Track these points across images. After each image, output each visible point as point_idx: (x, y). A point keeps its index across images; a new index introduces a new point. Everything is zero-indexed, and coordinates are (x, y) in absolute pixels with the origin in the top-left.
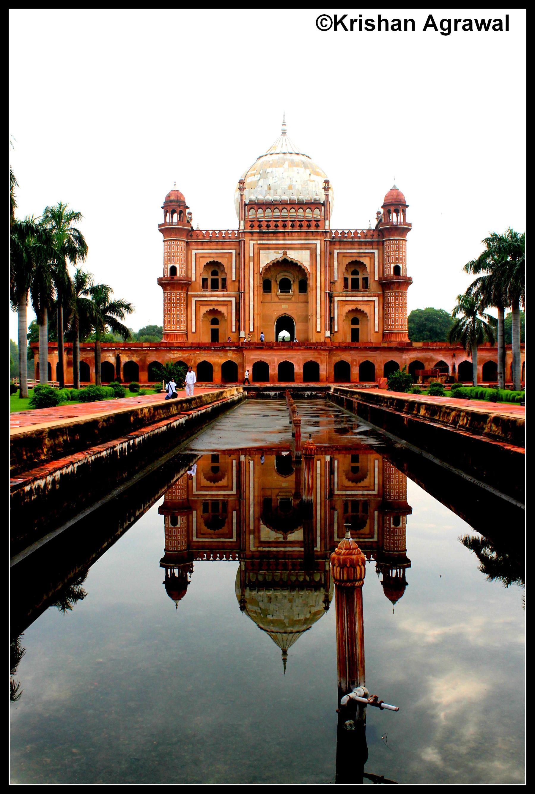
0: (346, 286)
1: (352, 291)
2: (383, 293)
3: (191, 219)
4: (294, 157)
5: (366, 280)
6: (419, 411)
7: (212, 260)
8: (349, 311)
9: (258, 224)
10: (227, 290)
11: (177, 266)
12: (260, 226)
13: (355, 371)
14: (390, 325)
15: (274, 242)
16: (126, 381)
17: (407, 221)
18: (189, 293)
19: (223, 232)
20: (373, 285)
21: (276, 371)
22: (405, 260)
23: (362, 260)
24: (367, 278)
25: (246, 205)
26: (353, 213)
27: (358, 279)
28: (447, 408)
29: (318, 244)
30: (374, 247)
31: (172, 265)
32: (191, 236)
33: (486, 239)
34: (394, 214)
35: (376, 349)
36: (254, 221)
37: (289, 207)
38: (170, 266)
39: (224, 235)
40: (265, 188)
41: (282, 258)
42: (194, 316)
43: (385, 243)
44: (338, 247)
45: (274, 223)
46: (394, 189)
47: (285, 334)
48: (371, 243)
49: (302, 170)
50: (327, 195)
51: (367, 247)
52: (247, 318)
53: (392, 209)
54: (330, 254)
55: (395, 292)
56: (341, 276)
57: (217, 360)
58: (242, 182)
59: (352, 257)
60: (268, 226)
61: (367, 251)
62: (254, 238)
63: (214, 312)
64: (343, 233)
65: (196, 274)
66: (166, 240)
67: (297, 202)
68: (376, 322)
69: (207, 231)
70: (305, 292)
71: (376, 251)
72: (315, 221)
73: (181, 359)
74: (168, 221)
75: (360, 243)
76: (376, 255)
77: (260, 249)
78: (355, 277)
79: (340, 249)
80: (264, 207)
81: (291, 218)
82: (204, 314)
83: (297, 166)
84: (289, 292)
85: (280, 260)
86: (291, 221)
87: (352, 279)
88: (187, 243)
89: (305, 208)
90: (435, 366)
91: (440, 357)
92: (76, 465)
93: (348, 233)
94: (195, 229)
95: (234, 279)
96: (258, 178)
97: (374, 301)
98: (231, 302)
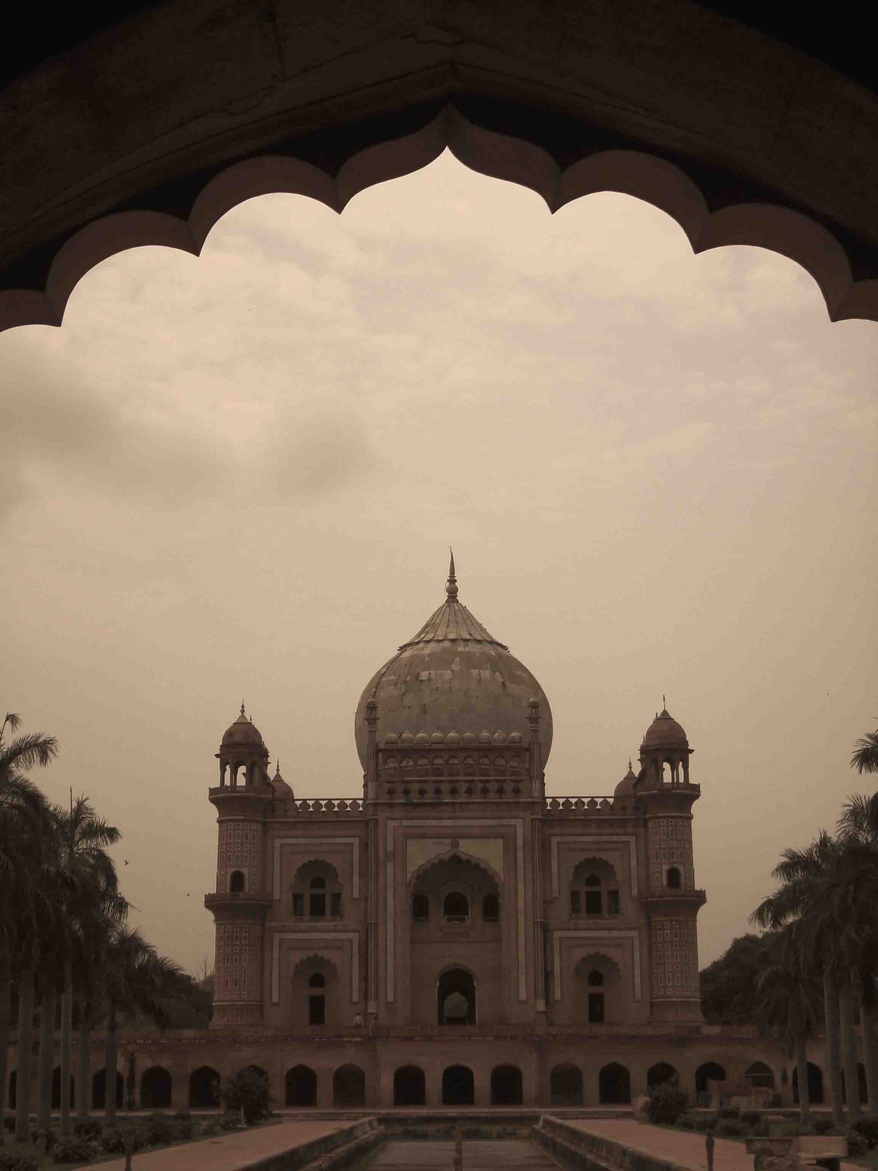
0: (575, 909)
8: (583, 959)
9: (400, 787)
11: (245, 871)
12: (407, 792)
13: (591, 1084)
15: (435, 822)
16: (144, 1106)
17: (692, 781)
18: (267, 924)
19: (336, 803)
21: (439, 1085)
23: (603, 856)
24: (617, 892)
25: (379, 750)
26: (586, 764)
27: (599, 894)
29: (520, 827)
30: (630, 830)
31: (234, 870)
33: (777, 870)
34: (666, 766)
38: (231, 871)
39: (336, 809)
42: (275, 970)
44: (557, 830)
46: (665, 718)
47: (456, 999)
48: (622, 823)
49: (486, 674)
50: (535, 731)
52: (381, 972)
54: (543, 845)
55: (671, 922)
57: (325, 1064)
60: (422, 792)
61: (615, 838)
63: (314, 961)
64: (567, 803)
68: (638, 981)
69: (305, 800)
70: (496, 920)
71: (632, 839)
72: (512, 781)
74: (227, 782)
75: (600, 823)
76: (633, 846)
77: (408, 837)
79: (561, 835)
82: (297, 966)
84: (463, 920)
85: (448, 856)
86: (466, 781)
88: (264, 824)
90: (747, 1073)
91: (757, 1056)
93: (576, 803)
95: (356, 895)
98: (350, 941)
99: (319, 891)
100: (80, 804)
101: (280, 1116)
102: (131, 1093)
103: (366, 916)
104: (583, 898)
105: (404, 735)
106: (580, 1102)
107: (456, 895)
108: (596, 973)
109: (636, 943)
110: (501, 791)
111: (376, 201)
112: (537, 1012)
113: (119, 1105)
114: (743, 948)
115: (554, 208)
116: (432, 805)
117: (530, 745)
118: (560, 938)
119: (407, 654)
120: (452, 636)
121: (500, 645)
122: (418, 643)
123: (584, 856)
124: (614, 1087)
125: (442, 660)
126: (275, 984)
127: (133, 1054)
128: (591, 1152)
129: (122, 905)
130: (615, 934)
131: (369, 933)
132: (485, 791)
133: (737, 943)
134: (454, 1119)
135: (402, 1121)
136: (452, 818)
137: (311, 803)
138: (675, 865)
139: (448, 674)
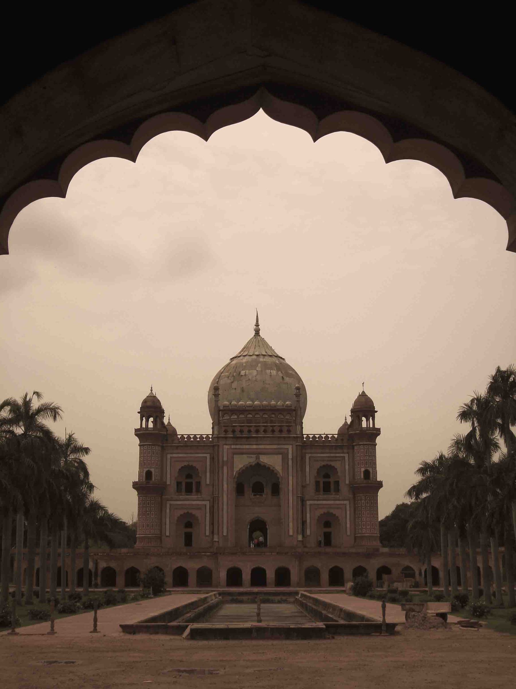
0: (317, 490)
1: (324, 494)
2: (354, 497)
4: (268, 359)
5: (337, 483)
7: (186, 464)
8: (321, 515)
10: (201, 493)
11: (152, 470)
12: (234, 431)
13: (325, 576)
14: (362, 528)
15: (247, 447)
16: (103, 586)
17: (376, 427)
18: (164, 497)
19: (198, 436)
20: (344, 489)
22: (375, 464)
23: (333, 464)
24: (338, 481)
25: (220, 411)
26: (324, 418)
27: (329, 483)
29: (290, 449)
30: (345, 451)
32: (167, 440)
33: (418, 470)
34: (364, 419)
36: (227, 426)
37: (261, 413)
39: (198, 440)
40: (239, 391)
41: (256, 462)
43: (356, 448)
45: (247, 429)
46: (363, 395)
48: (341, 447)
49: (274, 372)
50: (298, 401)
51: (338, 451)
53: (360, 415)
57: (192, 566)
59: (323, 461)
61: (338, 455)
62: (227, 443)
63: (187, 515)
64: (314, 437)
66: (143, 445)
67: (269, 408)
68: (348, 525)
69: (182, 435)
71: (346, 456)
72: (287, 426)
73: (157, 565)
74: (144, 426)
76: (347, 458)
77: (234, 454)
78: (327, 480)
79: (311, 453)
81: (263, 423)
83: (271, 369)
87: (324, 483)
88: (162, 447)
90: (403, 570)
91: (406, 562)
93: (318, 437)
95: (208, 482)
96: (232, 380)
97: (346, 504)
98: (206, 505)
99: (189, 480)
100: (70, 436)
101: (169, 591)
102: (96, 579)
103: (213, 494)
104: (322, 485)
105: (232, 403)
106: (319, 585)
107: (258, 482)
108: (328, 522)
109: (348, 507)
111: (225, 135)
112: (298, 541)
113: (90, 585)
114: (401, 509)
115: (315, 140)
116: (247, 438)
117: (295, 408)
118: (310, 505)
119: (234, 362)
120: (257, 353)
121: (281, 358)
122: (240, 356)
124: (336, 578)
125: (252, 365)
126: (168, 526)
127: (97, 561)
128: (324, 610)
129: (91, 487)
131: (214, 501)
132: (273, 431)
133: (398, 507)
134: (257, 593)
135: (230, 594)
136: (256, 445)
137: (186, 436)
138: (368, 468)
139: (255, 373)
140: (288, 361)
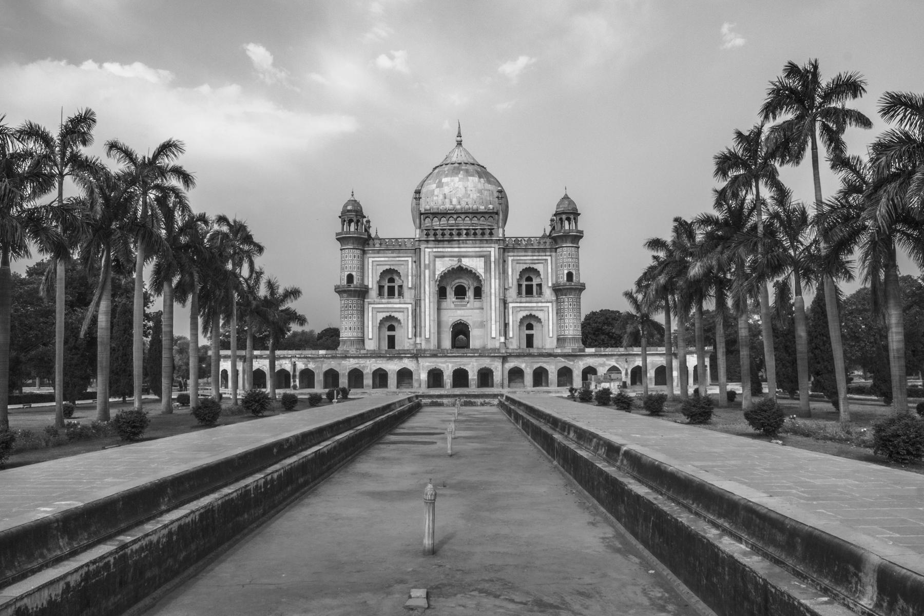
0: (519, 293)
3: (369, 227)
5: (540, 286)
6: (569, 433)
7: (388, 267)
11: (354, 274)
12: (435, 235)
13: (529, 378)
15: (449, 250)
16: (301, 388)
17: (579, 228)
22: (578, 266)
25: (421, 214)
26: (528, 220)
28: (591, 434)
29: (493, 251)
34: (566, 223)
35: (550, 355)
37: (463, 216)
38: (347, 273)
40: (441, 197)
43: (558, 250)
46: (566, 197)
48: (544, 250)
49: (476, 179)
52: (423, 325)
53: (564, 217)
56: (515, 283)
58: (418, 192)
60: (443, 235)
63: (390, 318)
65: (371, 281)
68: (551, 327)
71: (549, 258)
73: (356, 366)
76: (549, 262)
77: (436, 257)
80: (439, 216)
83: (473, 176)
89: (479, 216)
91: (612, 362)
92: (197, 513)
94: (373, 236)
95: (410, 286)
102: (294, 381)
110: (483, 234)
119: (436, 171)
123: (525, 266)
130: (540, 304)
140: (488, 170)
